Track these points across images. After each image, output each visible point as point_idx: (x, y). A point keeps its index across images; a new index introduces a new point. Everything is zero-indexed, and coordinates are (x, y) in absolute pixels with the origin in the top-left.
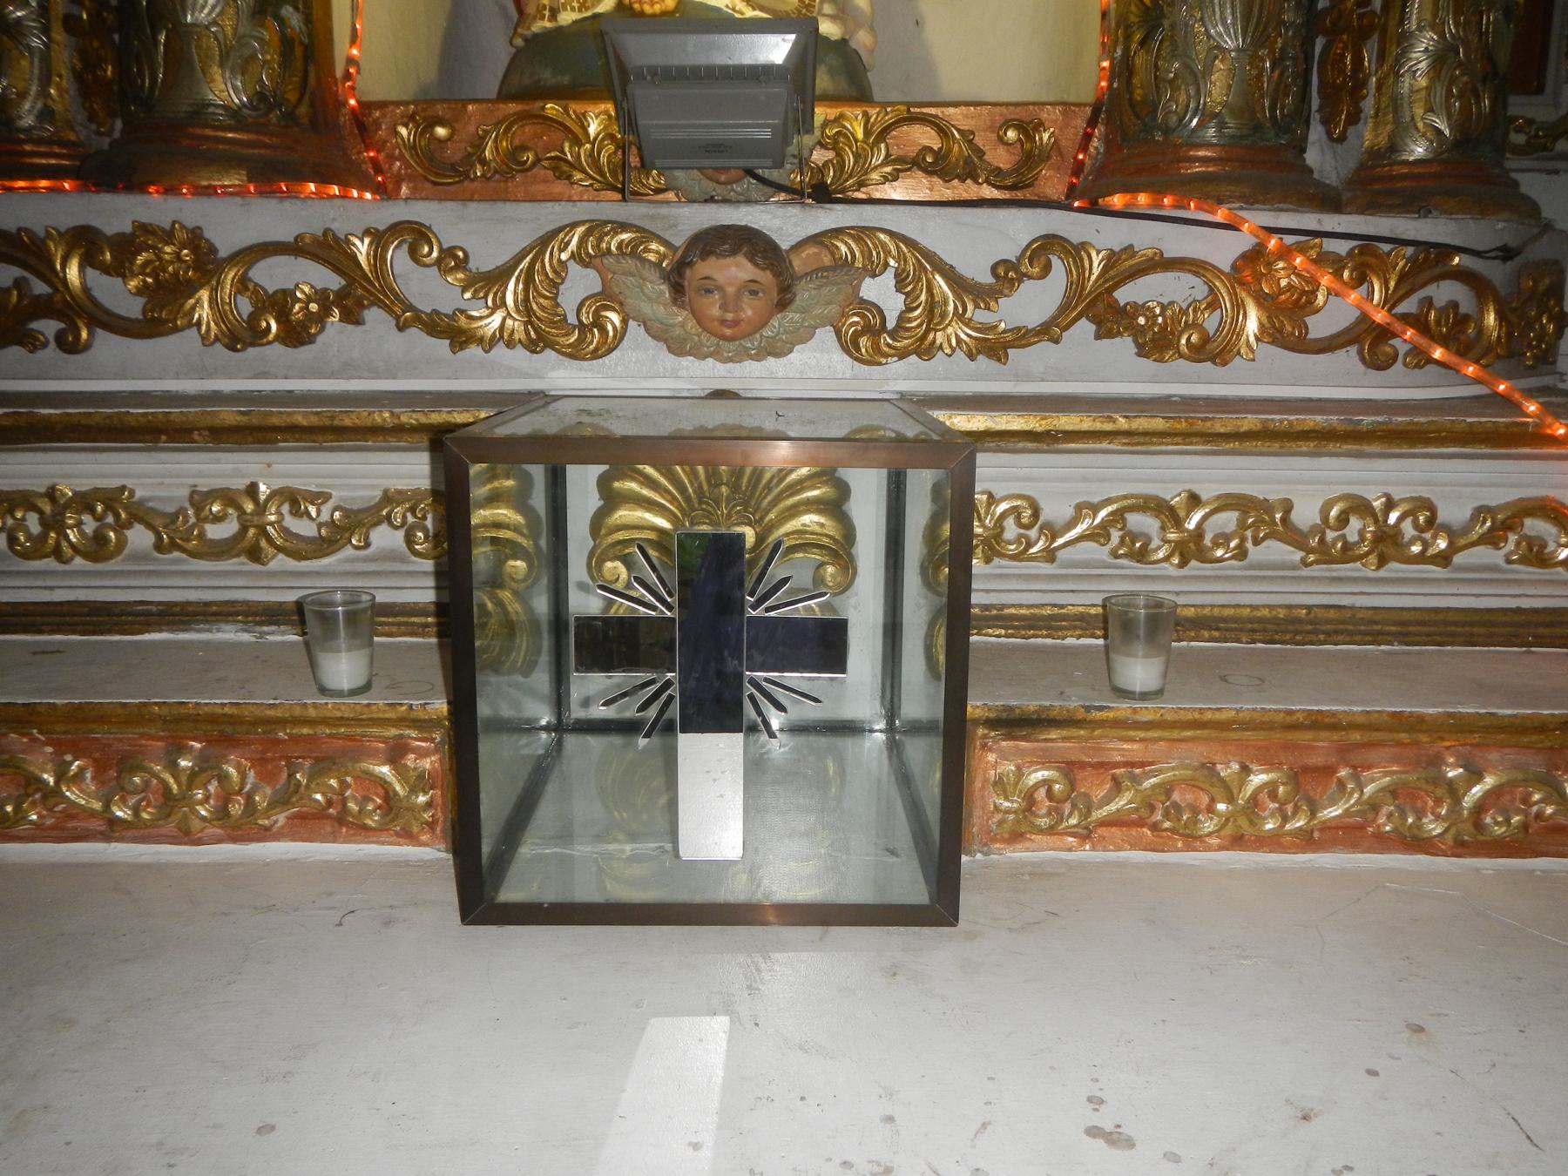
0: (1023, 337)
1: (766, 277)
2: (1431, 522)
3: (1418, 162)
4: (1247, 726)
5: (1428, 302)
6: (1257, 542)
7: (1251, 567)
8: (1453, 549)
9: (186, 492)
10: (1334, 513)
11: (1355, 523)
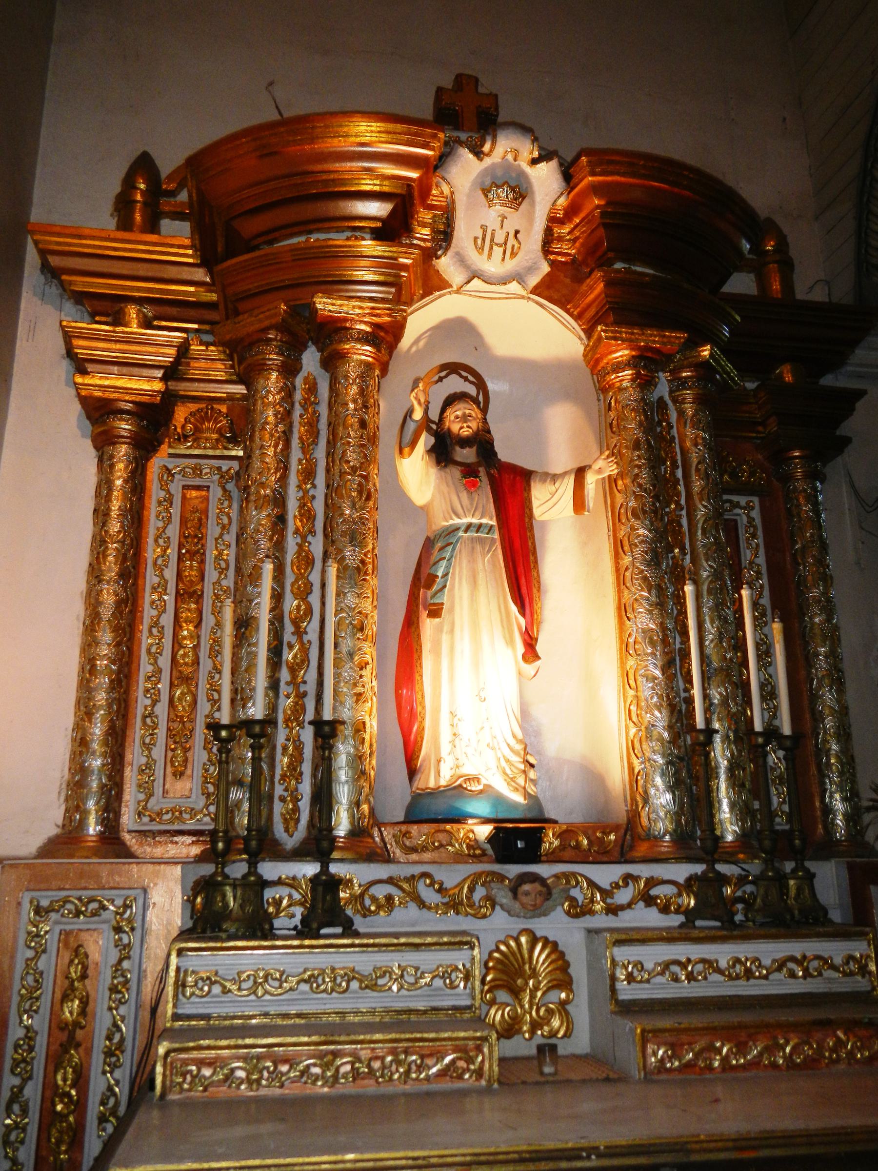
0: (622, 908)
1: (544, 889)
2: (760, 964)
3: (731, 842)
4: (723, 1028)
5: (744, 892)
6: (710, 974)
7: (712, 982)
8: (768, 974)
9: (371, 968)
10: (731, 963)
11: (738, 967)
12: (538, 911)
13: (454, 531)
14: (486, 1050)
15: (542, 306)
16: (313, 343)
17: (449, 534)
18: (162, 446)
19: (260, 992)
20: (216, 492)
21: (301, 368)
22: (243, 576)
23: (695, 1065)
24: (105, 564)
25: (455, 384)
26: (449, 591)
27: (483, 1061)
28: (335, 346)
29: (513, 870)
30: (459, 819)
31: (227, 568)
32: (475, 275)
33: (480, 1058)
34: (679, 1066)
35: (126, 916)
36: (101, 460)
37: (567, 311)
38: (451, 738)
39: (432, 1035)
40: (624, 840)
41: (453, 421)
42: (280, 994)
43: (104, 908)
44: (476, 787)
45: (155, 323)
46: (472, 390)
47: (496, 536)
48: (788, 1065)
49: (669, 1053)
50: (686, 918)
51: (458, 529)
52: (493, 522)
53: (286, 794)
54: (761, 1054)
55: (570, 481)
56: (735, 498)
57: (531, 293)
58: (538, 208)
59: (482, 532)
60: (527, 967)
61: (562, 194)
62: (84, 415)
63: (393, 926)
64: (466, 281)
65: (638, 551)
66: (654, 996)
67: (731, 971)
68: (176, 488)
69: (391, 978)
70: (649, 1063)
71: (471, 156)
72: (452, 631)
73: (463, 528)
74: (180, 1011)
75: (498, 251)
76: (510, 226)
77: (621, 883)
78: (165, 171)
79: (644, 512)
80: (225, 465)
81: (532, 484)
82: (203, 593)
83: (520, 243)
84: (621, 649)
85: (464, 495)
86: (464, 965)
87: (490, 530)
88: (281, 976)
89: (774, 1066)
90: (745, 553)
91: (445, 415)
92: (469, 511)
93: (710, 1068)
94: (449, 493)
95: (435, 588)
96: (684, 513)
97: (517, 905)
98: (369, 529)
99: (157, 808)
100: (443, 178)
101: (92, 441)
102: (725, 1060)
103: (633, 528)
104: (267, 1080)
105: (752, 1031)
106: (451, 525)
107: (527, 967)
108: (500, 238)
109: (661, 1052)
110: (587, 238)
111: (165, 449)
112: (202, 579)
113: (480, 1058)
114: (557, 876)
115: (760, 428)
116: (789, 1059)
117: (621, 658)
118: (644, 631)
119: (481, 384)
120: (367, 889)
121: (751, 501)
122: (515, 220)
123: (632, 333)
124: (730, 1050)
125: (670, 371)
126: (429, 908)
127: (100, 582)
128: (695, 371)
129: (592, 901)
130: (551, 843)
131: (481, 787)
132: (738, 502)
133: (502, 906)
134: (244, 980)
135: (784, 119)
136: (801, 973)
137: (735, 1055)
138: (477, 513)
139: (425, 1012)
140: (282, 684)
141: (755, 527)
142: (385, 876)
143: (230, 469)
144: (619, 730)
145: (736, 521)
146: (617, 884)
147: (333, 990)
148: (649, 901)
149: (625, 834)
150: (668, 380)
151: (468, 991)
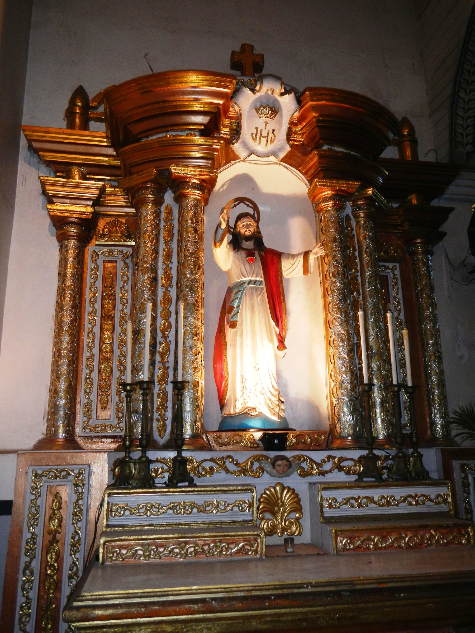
0: (327, 472)
1: (288, 463)
2: (394, 499)
3: (382, 439)
5: (388, 464)
6: (369, 504)
7: (370, 508)
8: (398, 503)
9: (203, 502)
11: (383, 500)
12: (285, 474)
13: (243, 284)
14: (259, 541)
15: (286, 168)
16: (170, 189)
17: (240, 285)
18: (92, 240)
19: (149, 513)
20: (121, 264)
21: (164, 201)
22: (136, 308)
23: (361, 547)
24: (65, 301)
25: (242, 208)
27: (258, 546)
28: (181, 191)
29: (273, 454)
30: (246, 429)
31: (127, 303)
32: (252, 152)
33: (256, 545)
34: (353, 548)
35: (80, 478)
36: (61, 248)
37: (299, 171)
38: (242, 389)
39: (233, 534)
40: (328, 439)
41: (242, 228)
42: (159, 515)
43: (69, 474)
44: (254, 413)
45: (88, 176)
46: (251, 211)
47: (264, 286)
48: (406, 547)
49: (349, 541)
50: (358, 477)
51: (244, 283)
52: (262, 279)
53: (159, 417)
54: (393, 542)
55: (301, 258)
56: (387, 264)
60: (280, 501)
61: (296, 111)
62: (52, 224)
63: (214, 482)
64: (247, 155)
65: (335, 294)
66: (342, 515)
67: (380, 502)
68: (100, 262)
69: (213, 507)
70: (339, 546)
71: (249, 92)
72: (242, 335)
73: (247, 283)
74: (110, 523)
75: (264, 140)
76: (270, 128)
77: (326, 460)
78: (91, 96)
79: (339, 274)
80: (125, 250)
81: (282, 260)
82: (115, 315)
83: (275, 136)
84: (327, 344)
85: (247, 266)
86: (248, 500)
87: (260, 284)
88: (159, 506)
89: (400, 547)
90: (392, 293)
91: (237, 224)
92: (250, 274)
93: (368, 549)
95: (233, 313)
96: (359, 274)
97: (275, 471)
98: (200, 284)
99: (93, 425)
100: (235, 103)
101: (57, 238)
102: (376, 545)
103: (333, 283)
104: (153, 555)
105: (389, 530)
106: (241, 281)
107: (280, 501)
108: (264, 134)
109: (344, 541)
110: (310, 132)
111: (94, 242)
112: (114, 308)
113: (256, 545)
114: (294, 457)
115: (400, 228)
116: (407, 544)
117: (327, 348)
118: (338, 334)
119: (256, 208)
120: (200, 464)
121: (395, 266)
122: (272, 124)
123: (332, 183)
124: (378, 540)
125: (352, 201)
126: (231, 473)
127: (62, 311)
128: (365, 201)
129: (312, 469)
130: (292, 441)
131: (257, 413)
132: (388, 266)
133: (267, 472)
134: (141, 508)
135: (413, 64)
136: (414, 503)
137: (381, 542)
138: (254, 275)
139: (229, 523)
140: (157, 363)
141: (397, 279)
142: (209, 458)
143: (127, 252)
144: (326, 384)
145: (387, 276)
146: (324, 460)
147: (184, 513)
148: (340, 469)
149: (329, 436)
150: (351, 206)
151: (250, 513)
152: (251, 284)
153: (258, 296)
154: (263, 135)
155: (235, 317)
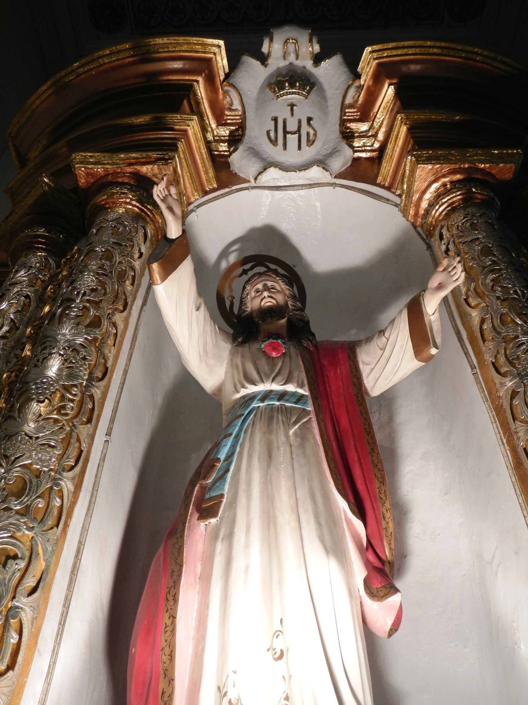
26: (232, 478)
47: (310, 408)
57: (335, 177)
58: (330, 103)
59: (287, 401)
72: (230, 536)
75: (292, 139)
76: (301, 112)
94: (243, 363)
106: (243, 397)
138: (279, 379)
152: (272, 399)
153: (288, 426)
154: (288, 129)
155: (217, 484)
